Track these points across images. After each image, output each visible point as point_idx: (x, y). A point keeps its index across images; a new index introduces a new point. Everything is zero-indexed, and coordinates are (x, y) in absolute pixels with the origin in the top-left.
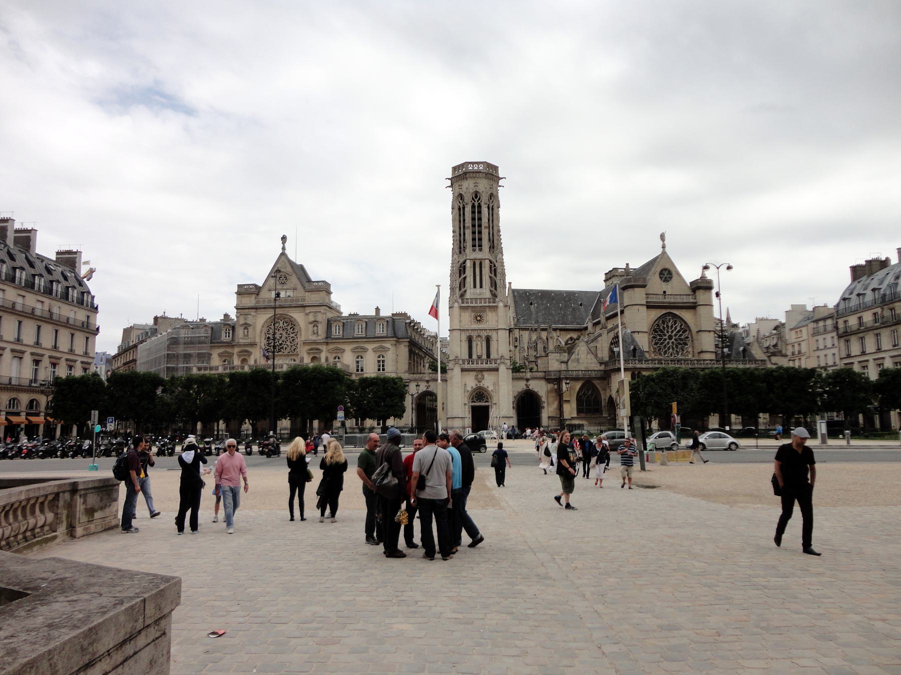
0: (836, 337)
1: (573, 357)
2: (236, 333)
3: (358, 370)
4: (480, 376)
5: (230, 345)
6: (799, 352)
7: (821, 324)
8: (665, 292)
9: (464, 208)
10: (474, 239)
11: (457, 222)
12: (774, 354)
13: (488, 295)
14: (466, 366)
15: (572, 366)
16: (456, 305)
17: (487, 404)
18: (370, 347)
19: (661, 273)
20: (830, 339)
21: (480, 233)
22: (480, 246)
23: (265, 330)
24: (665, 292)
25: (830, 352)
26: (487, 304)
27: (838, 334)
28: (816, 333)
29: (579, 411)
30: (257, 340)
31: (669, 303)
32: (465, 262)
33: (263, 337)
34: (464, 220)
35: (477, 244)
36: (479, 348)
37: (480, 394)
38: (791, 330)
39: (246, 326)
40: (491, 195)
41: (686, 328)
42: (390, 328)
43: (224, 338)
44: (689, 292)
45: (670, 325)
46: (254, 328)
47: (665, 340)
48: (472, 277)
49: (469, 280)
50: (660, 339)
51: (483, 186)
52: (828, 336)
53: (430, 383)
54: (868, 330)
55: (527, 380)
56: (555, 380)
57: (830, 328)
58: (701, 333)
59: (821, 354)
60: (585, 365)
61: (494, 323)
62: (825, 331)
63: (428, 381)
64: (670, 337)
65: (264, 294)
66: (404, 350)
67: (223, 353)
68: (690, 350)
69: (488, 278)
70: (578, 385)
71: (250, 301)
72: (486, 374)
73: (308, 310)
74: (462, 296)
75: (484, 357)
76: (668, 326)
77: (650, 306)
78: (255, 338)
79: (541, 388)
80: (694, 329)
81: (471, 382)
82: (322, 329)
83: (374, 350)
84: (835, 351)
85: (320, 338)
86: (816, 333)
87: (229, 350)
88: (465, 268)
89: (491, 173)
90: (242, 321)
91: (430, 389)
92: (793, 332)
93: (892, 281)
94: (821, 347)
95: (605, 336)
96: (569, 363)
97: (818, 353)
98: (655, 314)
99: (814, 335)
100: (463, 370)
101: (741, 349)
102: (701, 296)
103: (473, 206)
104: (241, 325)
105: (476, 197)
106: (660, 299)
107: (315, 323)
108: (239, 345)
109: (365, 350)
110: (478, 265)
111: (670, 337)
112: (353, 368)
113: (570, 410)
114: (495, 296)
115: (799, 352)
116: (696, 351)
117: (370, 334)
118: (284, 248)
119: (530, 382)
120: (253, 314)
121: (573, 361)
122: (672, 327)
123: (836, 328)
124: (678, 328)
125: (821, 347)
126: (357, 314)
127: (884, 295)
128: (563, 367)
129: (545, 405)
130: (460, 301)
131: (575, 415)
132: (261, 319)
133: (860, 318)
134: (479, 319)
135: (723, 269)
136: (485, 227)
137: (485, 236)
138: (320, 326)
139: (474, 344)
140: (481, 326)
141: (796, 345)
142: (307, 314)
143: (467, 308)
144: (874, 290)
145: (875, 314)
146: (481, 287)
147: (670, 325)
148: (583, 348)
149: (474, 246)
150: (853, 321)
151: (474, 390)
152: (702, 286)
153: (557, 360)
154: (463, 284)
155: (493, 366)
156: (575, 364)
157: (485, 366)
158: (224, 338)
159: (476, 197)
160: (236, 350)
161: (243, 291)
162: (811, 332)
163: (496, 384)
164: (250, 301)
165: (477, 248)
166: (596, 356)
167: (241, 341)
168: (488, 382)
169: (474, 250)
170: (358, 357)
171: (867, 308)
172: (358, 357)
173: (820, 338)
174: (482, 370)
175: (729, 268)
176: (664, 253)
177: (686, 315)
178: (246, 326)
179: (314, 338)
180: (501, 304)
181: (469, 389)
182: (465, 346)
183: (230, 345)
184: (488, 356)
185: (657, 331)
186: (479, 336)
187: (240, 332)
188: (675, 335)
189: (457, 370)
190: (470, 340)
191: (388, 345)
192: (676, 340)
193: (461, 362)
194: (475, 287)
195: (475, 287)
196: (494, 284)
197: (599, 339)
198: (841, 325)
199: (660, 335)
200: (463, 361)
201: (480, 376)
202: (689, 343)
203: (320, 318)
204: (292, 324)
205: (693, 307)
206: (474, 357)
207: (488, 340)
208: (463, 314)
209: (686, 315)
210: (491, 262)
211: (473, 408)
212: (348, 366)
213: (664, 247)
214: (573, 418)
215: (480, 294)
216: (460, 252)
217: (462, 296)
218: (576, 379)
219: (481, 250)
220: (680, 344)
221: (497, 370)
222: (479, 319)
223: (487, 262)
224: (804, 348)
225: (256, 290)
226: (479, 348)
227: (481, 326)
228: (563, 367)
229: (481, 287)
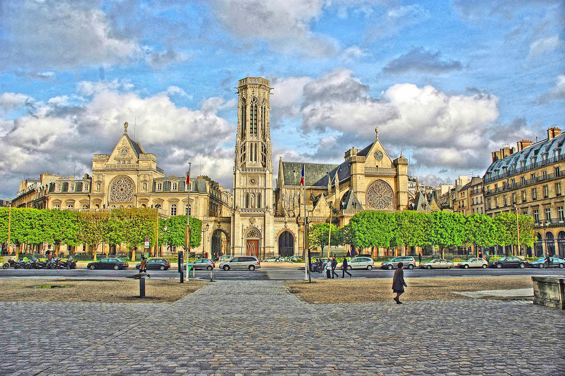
6: (463, 206)
8: (377, 166)
9: (246, 107)
12: (445, 207)
14: (244, 213)
15: (315, 214)
18: (181, 199)
19: (376, 154)
27: (484, 195)
35: (254, 131)
36: (253, 201)
37: (254, 232)
38: (458, 192)
46: (104, 184)
49: (248, 155)
52: (479, 196)
53: (221, 224)
54: (500, 193)
55: (286, 223)
57: (480, 191)
60: (324, 213)
63: (219, 223)
72: (257, 219)
73: (140, 173)
77: (367, 176)
79: (293, 228)
81: (246, 223)
82: (150, 185)
84: (483, 206)
86: (472, 194)
91: (221, 228)
92: (460, 193)
93: (514, 162)
94: (475, 203)
98: (369, 181)
105: (254, 100)
106: (373, 172)
107: (145, 182)
110: (254, 146)
114: (264, 166)
119: (287, 224)
121: (316, 211)
123: (483, 191)
127: (509, 171)
129: (297, 240)
130: (241, 169)
132: (108, 179)
133: (496, 185)
134: (253, 182)
141: (461, 202)
143: (245, 174)
144: (503, 168)
145: (504, 183)
146: (256, 160)
150: (492, 187)
156: (317, 213)
157: (256, 213)
159: (254, 100)
168: (258, 223)
171: (500, 178)
179: (143, 191)
184: (259, 206)
185: (371, 190)
187: (95, 187)
193: (240, 210)
194: (251, 160)
195: (251, 160)
196: (264, 159)
198: (486, 190)
200: (242, 210)
203: (147, 178)
204: (131, 181)
216: (242, 137)
223: (260, 143)
224: (465, 204)
226: (253, 201)
229: (256, 160)
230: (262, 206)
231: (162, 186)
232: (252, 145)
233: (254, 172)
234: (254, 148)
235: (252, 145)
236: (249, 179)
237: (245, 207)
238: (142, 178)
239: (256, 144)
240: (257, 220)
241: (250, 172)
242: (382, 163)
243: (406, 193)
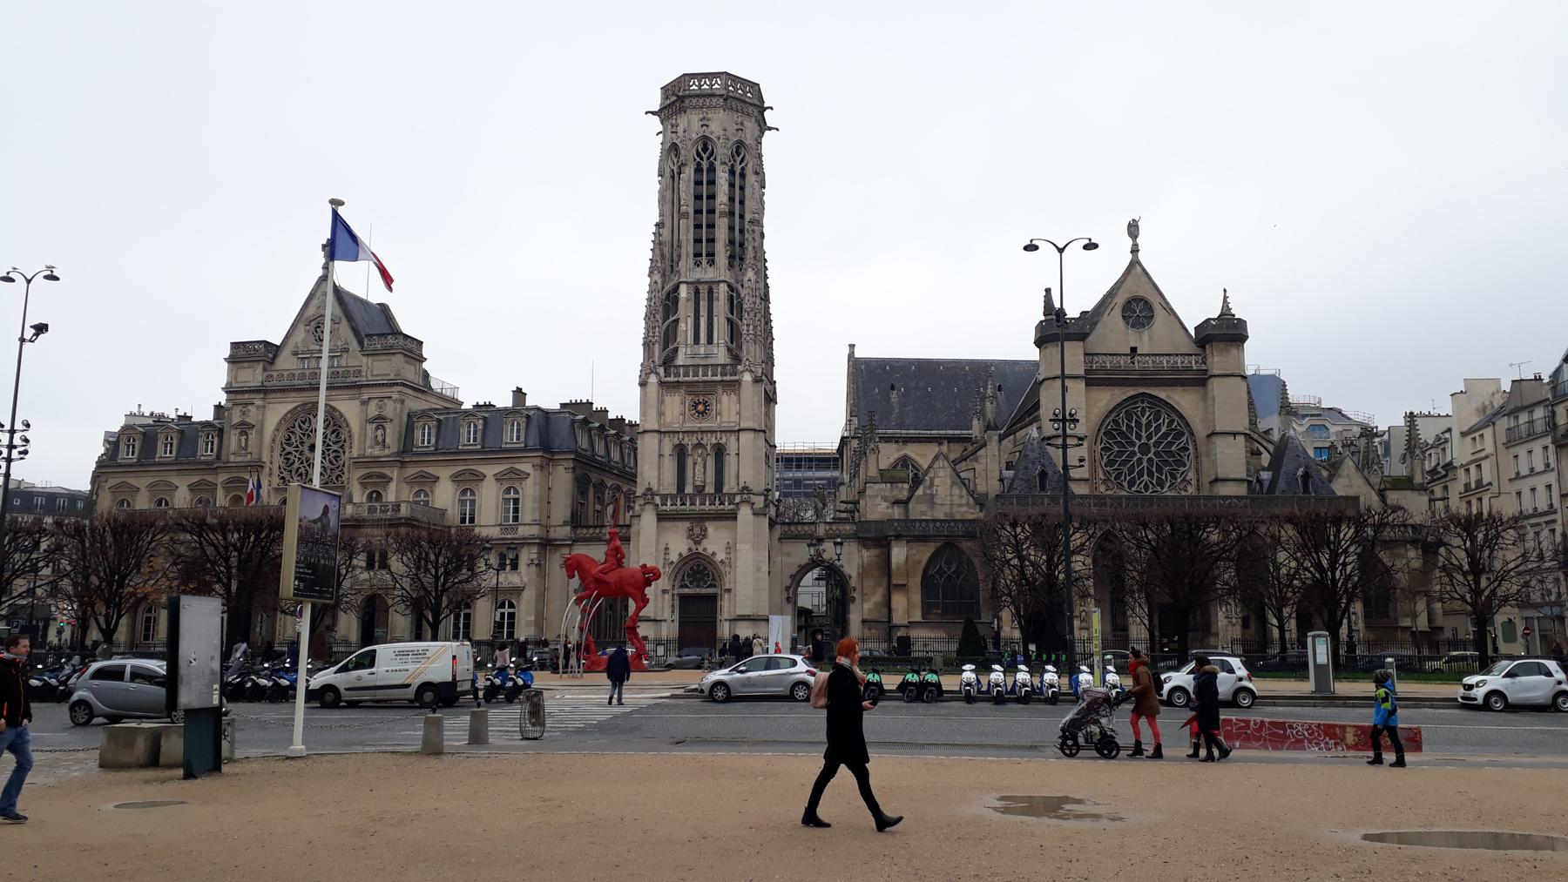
0: (1551, 448)
1: (920, 492)
2: (225, 443)
3: (463, 520)
4: (697, 531)
5: (210, 467)
6: (1479, 483)
7: (1524, 418)
8: (1134, 350)
10: (698, 241)
11: (668, 206)
13: (722, 356)
14: (668, 507)
15: (918, 510)
16: (653, 379)
17: (711, 591)
18: (490, 470)
20: (1538, 453)
21: (711, 226)
22: (711, 255)
23: (281, 435)
24: (1134, 350)
25: (1540, 482)
26: (719, 378)
28: (1513, 440)
29: (926, 611)
30: (266, 458)
31: (1143, 371)
32: (676, 288)
36: (700, 472)
38: (1464, 434)
39: (244, 428)
40: (739, 147)
41: (1180, 428)
42: (534, 432)
43: (205, 452)
44: (1193, 349)
45: (1144, 421)
46: (261, 432)
47: (1134, 453)
48: (690, 321)
49: (685, 327)
50: (1121, 453)
51: (720, 124)
52: (1537, 446)
55: (820, 540)
56: (878, 538)
57: (1540, 427)
58: (1214, 438)
59: (1524, 486)
60: (947, 509)
61: (734, 418)
62: (1532, 436)
64: (1145, 449)
65: (286, 362)
66: (563, 478)
67: (199, 483)
68: (1191, 475)
69: (723, 322)
70: (925, 552)
71: (253, 376)
72: (711, 527)
74: (668, 362)
75: (710, 489)
76: (1138, 424)
77: (1093, 380)
78: (260, 453)
80: (1200, 430)
81: (678, 543)
83: (499, 478)
85: (387, 452)
87: (210, 478)
88: (676, 301)
89: (744, 100)
90: (236, 419)
94: (1524, 471)
95: (993, 446)
96: (911, 505)
97: (1518, 485)
98: (1106, 399)
99: (1509, 444)
100: (662, 518)
101: (1300, 472)
102: (1217, 361)
103: (699, 170)
104: (236, 427)
107: (379, 421)
108: (227, 467)
109: (481, 478)
111: (1145, 449)
112: (453, 515)
113: (906, 608)
114: (737, 359)
115: (1479, 483)
116: (1205, 480)
117: (490, 443)
120: (258, 402)
122: (1149, 425)
123: (1552, 425)
124: (1164, 429)
125: (1524, 471)
126: (491, 405)
128: (897, 513)
130: (661, 371)
131: (917, 616)
134: (702, 409)
135: (1075, 250)
136: (722, 214)
137: (721, 233)
138: (388, 426)
139: (689, 461)
140: (705, 425)
141: (1473, 468)
142: (365, 403)
146: (710, 341)
147: (1144, 421)
148: (941, 473)
149: (697, 255)
151: (684, 560)
152: (1226, 332)
153: (885, 499)
154: (669, 336)
155: (727, 507)
157: (707, 507)
158: (205, 452)
159: (705, 149)
160: (222, 477)
161: (242, 354)
162: (1502, 438)
163: (730, 548)
164: (253, 376)
165: (704, 260)
166: (971, 493)
167: (232, 458)
168: (715, 542)
169: (698, 264)
170: (464, 492)
172: (464, 492)
173: (1521, 451)
174: (702, 518)
175: (1090, 246)
176: (1135, 263)
177: (1184, 401)
178: (244, 428)
179: (377, 452)
180: (747, 377)
181: (674, 558)
182: (670, 466)
183: (210, 467)
186: (699, 445)
187: (233, 440)
188: (1157, 444)
189: (648, 520)
190: (681, 452)
191: (526, 467)
192: (1157, 454)
193: (658, 500)
194: (697, 340)
195: (697, 340)
197: (982, 452)
199: (1119, 444)
200: (664, 498)
201: (697, 531)
202: (1190, 462)
203: (390, 409)
205: (1199, 380)
206: (689, 489)
207: (720, 451)
208: (668, 399)
209: (1184, 401)
210: (729, 286)
211: (683, 598)
212: (443, 512)
214: (911, 625)
215: (707, 356)
217: (668, 362)
218: (922, 538)
219: (712, 263)
220: (1166, 462)
221: (732, 516)
222: (702, 409)
223: (723, 288)
226: (700, 472)
228: (897, 513)
229: (710, 341)
230: (730, 486)
231: (433, 432)
232: (697, 292)
233: (701, 378)
234: (703, 304)
235: (697, 292)
236: (689, 399)
238: (373, 410)
239: (710, 292)
240: (710, 530)
241: (690, 378)
242: (1151, 339)
243: (1241, 439)
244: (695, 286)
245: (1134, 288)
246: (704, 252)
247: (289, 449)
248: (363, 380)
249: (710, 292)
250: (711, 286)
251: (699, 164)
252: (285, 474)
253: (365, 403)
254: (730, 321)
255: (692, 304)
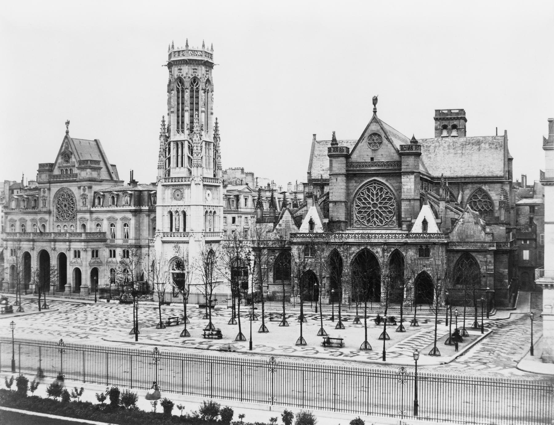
14: (165, 239)
32: (169, 144)
33: (55, 207)
34: (183, 104)
36: (178, 223)
75: (181, 230)
111: (375, 205)
118: (67, 132)
140: (180, 203)
142: (79, 188)
186: (177, 212)
206: (174, 230)
210: (189, 143)
213: (375, 112)
223: (186, 143)
225: (51, 166)
226: (178, 223)
227: (180, 203)
235: (177, 145)
237: (168, 230)
244: (177, 143)
245: (374, 128)
246: (180, 128)
247: (59, 206)
248: (78, 179)
249: (182, 145)
250: (182, 142)
251: (178, 89)
252: (58, 216)
253: (79, 188)
254: (189, 157)
255: (175, 150)
